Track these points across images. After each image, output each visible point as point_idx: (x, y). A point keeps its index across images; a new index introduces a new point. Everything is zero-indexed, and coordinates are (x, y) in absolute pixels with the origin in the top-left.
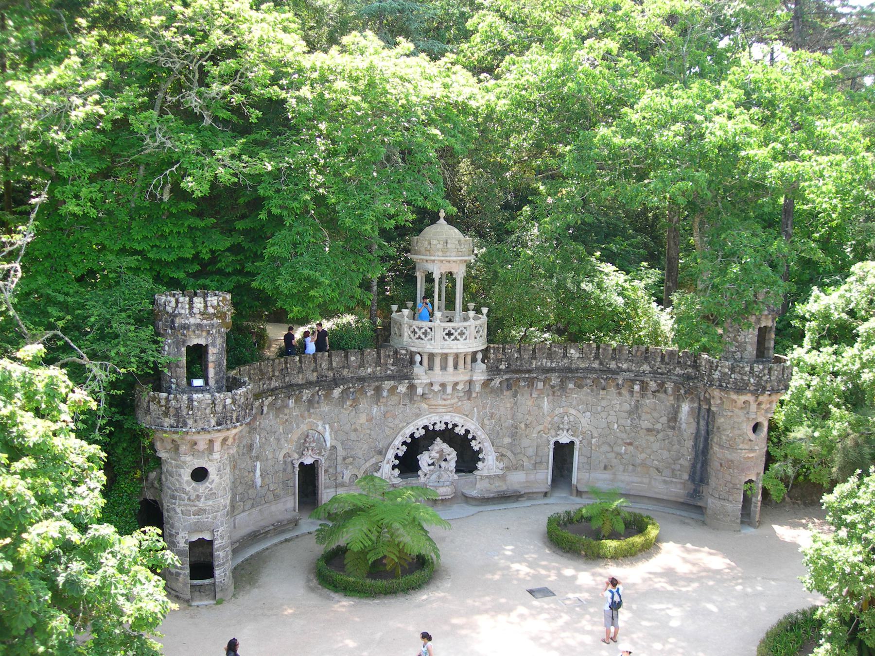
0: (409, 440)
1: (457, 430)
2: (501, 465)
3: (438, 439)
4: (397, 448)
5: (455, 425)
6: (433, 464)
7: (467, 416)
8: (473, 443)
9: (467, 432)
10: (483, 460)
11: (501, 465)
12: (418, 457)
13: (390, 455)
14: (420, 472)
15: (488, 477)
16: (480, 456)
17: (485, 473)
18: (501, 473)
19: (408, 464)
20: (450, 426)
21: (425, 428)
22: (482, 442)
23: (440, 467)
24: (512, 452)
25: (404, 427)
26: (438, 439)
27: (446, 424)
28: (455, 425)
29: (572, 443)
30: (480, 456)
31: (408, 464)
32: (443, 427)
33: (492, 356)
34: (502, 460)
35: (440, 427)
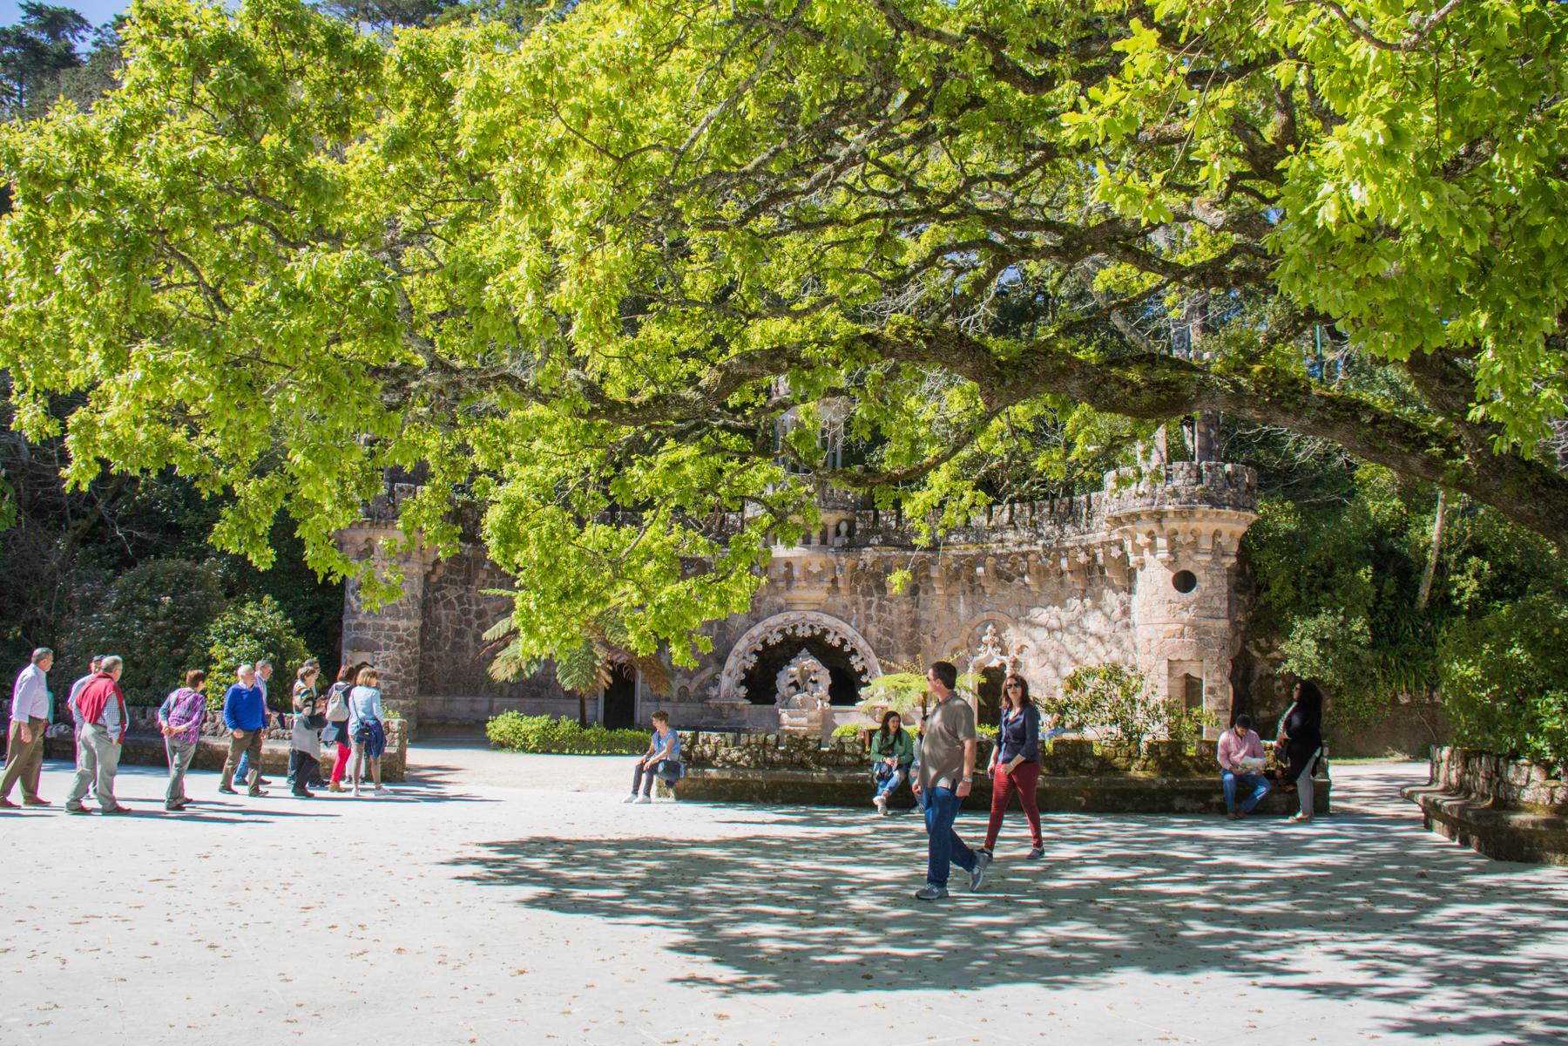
0: (760, 648)
1: (829, 638)
3: (805, 651)
4: (740, 659)
5: (825, 632)
6: (795, 684)
7: (841, 618)
9: (844, 642)
20: (817, 632)
22: (864, 658)
25: (750, 627)
26: (805, 651)
27: (812, 627)
28: (825, 632)
29: (1003, 665)
32: (808, 633)
33: (859, 526)
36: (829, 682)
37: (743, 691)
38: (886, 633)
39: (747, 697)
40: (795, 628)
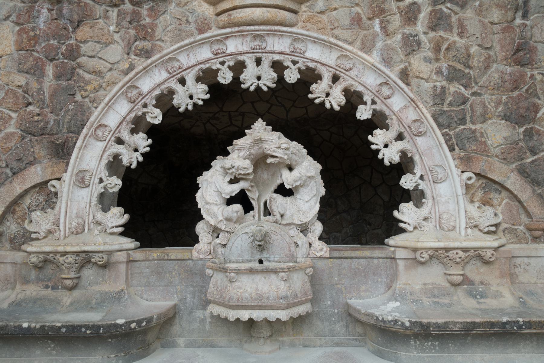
0: (156, 117)
1: (318, 91)
2: (487, 217)
3: (259, 125)
4: (111, 138)
5: (310, 77)
7: (351, 44)
8: (378, 138)
9: (353, 99)
10: (415, 196)
11: (487, 217)
12: (200, 180)
13: (91, 156)
14: (200, 228)
15: (438, 256)
16: (407, 182)
17: (428, 239)
18: (490, 242)
19: (158, 201)
20: (292, 76)
21: (207, 76)
22: (409, 134)
23: (267, 212)
24: (522, 172)
25: (132, 68)
26: (259, 125)
27: (278, 66)
28: (310, 77)
30: (407, 182)
31: (158, 201)
32: (269, 78)
34: (486, 202)
35: (258, 77)
36: (318, 189)
37: (117, 217)
38: (453, 75)
39: (128, 231)
40: (239, 67)
